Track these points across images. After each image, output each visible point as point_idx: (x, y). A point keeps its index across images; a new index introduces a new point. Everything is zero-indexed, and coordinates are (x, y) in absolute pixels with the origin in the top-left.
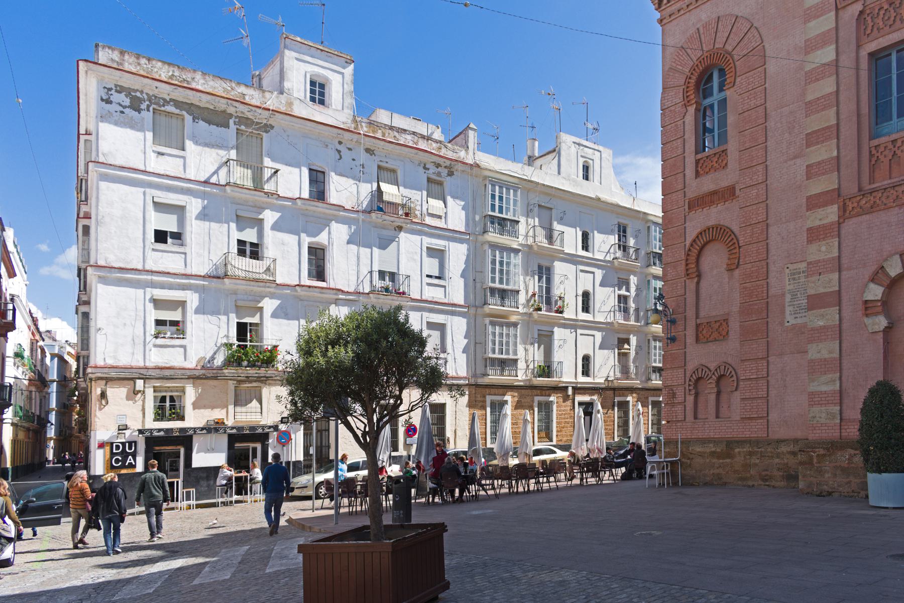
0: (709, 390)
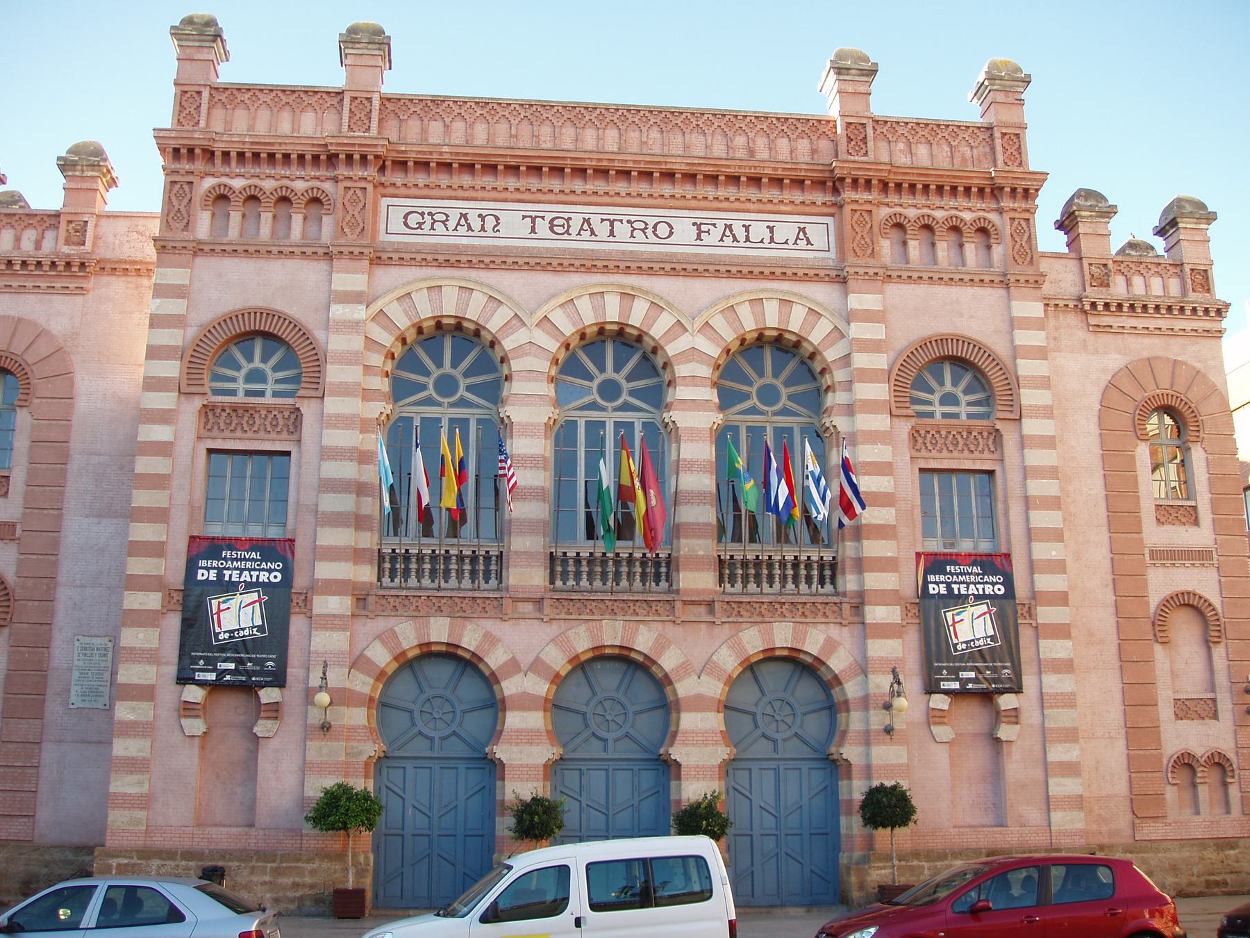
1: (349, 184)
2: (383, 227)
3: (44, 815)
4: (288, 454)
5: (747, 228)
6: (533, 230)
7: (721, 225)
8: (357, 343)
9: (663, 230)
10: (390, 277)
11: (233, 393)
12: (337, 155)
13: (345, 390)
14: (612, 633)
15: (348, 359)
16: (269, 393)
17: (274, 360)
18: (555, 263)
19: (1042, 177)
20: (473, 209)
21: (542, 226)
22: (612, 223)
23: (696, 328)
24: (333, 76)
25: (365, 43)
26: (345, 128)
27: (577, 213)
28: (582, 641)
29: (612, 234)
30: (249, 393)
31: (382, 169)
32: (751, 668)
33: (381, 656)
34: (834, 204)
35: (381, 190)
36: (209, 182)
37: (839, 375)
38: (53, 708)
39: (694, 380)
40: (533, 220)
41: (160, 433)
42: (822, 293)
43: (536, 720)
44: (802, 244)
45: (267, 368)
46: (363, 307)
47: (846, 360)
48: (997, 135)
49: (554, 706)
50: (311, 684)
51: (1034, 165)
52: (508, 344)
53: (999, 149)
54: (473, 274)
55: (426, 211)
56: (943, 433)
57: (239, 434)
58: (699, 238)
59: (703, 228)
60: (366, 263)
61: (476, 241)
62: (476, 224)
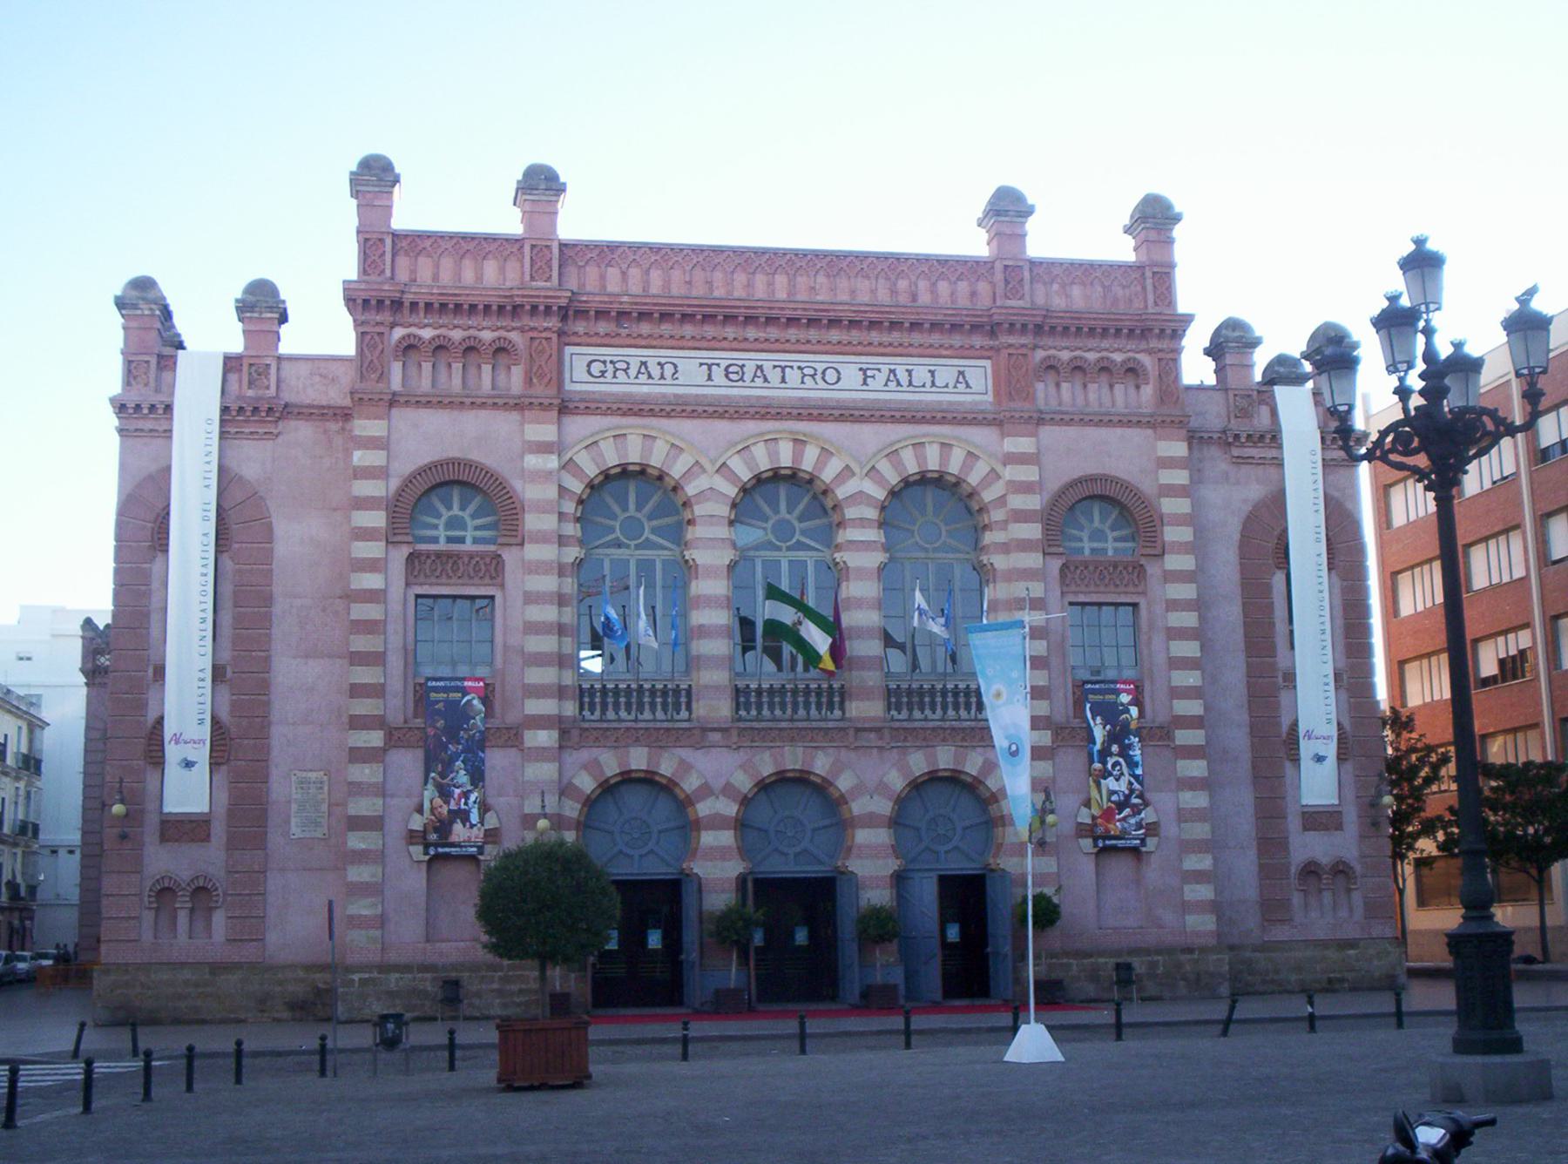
0: (183, 903)
1: (535, 334)
2: (567, 375)
3: (272, 938)
4: (492, 598)
5: (910, 372)
6: (710, 378)
7: (885, 369)
8: (552, 492)
9: (831, 376)
10: (579, 427)
11: (435, 540)
12: (522, 306)
13: (541, 538)
14: (793, 758)
15: (542, 508)
16: (469, 540)
17: (472, 508)
18: (732, 410)
19: (1187, 319)
20: (653, 356)
21: (718, 374)
22: (783, 369)
23: (858, 467)
24: (510, 223)
25: (541, 186)
26: (527, 278)
27: (750, 360)
28: (767, 767)
29: (783, 380)
30: (450, 540)
31: (564, 318)
32: (918, 786)
33: (587, 783)
34: (991, 348)
35: (567, 340)
36: (399, 333)
37: (997, 515)
38: (275, 839)
39: (862, 523)
40: (710, 367)
41: (372, 581)
42: (981, 436)
43: (727, 838)
44: (961, 387)
45: (466, 515)
46: (554, 457)
47: (1002, 501)
48: (1148, 274)
49: (741, 825)
50: (527, 811)
51: (1182, 308)
52: (691, 490)
53: (1150, 288)
54: (654, 421)
55: (608, 359)
56: (1091, 568)
57: (444, 580)
58: (865, 383)
59: (869, 373)
60: (555, 413)
61: (657, 390)
62: (656, 372)
